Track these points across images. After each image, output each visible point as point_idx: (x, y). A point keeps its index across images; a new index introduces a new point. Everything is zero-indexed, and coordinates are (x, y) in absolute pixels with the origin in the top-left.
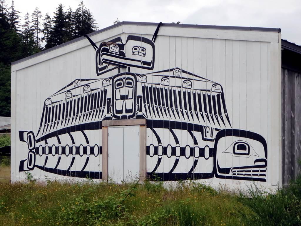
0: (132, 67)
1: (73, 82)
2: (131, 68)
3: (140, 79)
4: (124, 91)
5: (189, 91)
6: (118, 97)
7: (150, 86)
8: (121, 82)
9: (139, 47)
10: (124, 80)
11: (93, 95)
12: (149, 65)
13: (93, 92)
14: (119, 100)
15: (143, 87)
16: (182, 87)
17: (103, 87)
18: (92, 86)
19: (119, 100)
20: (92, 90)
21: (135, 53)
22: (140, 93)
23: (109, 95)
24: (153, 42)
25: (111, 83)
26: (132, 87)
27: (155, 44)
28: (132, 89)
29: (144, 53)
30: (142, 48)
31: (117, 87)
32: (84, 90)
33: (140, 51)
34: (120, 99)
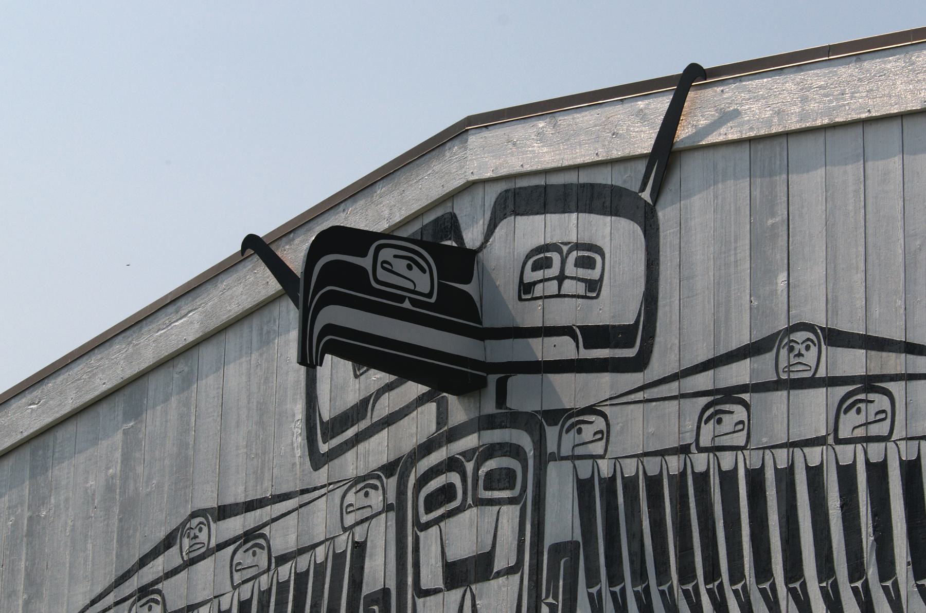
0: (520, 376)
1: (177, 529)
2: (516, 382)
3: (569, 440)
4: (464, 534)
5: (876, 452)
6: (431, 575)
7: (630, 468)
8: (454, 478)
9: (565, 249)
10: (469, 466)
11: (283, 587)
12: (623, 346)
13: (285, 571)
14: (436, 591)
15: (584, 488)
16: (831, 440)
17: (345, 530)
18: (283, 538)
19: (441, 595)
20: (282, 559)
21: (538, 290)
22: (562, 521)
23: (378, 571)
24: (649, 201)
25: (392, 499)
26: (511, 501)
27: (666, 215)
28: (515, 510)
29: (595, 274)
30: (578, 246)
31: (424, 518)
32: (234, 568)
33: (567, 273)
34: (442, 586)
